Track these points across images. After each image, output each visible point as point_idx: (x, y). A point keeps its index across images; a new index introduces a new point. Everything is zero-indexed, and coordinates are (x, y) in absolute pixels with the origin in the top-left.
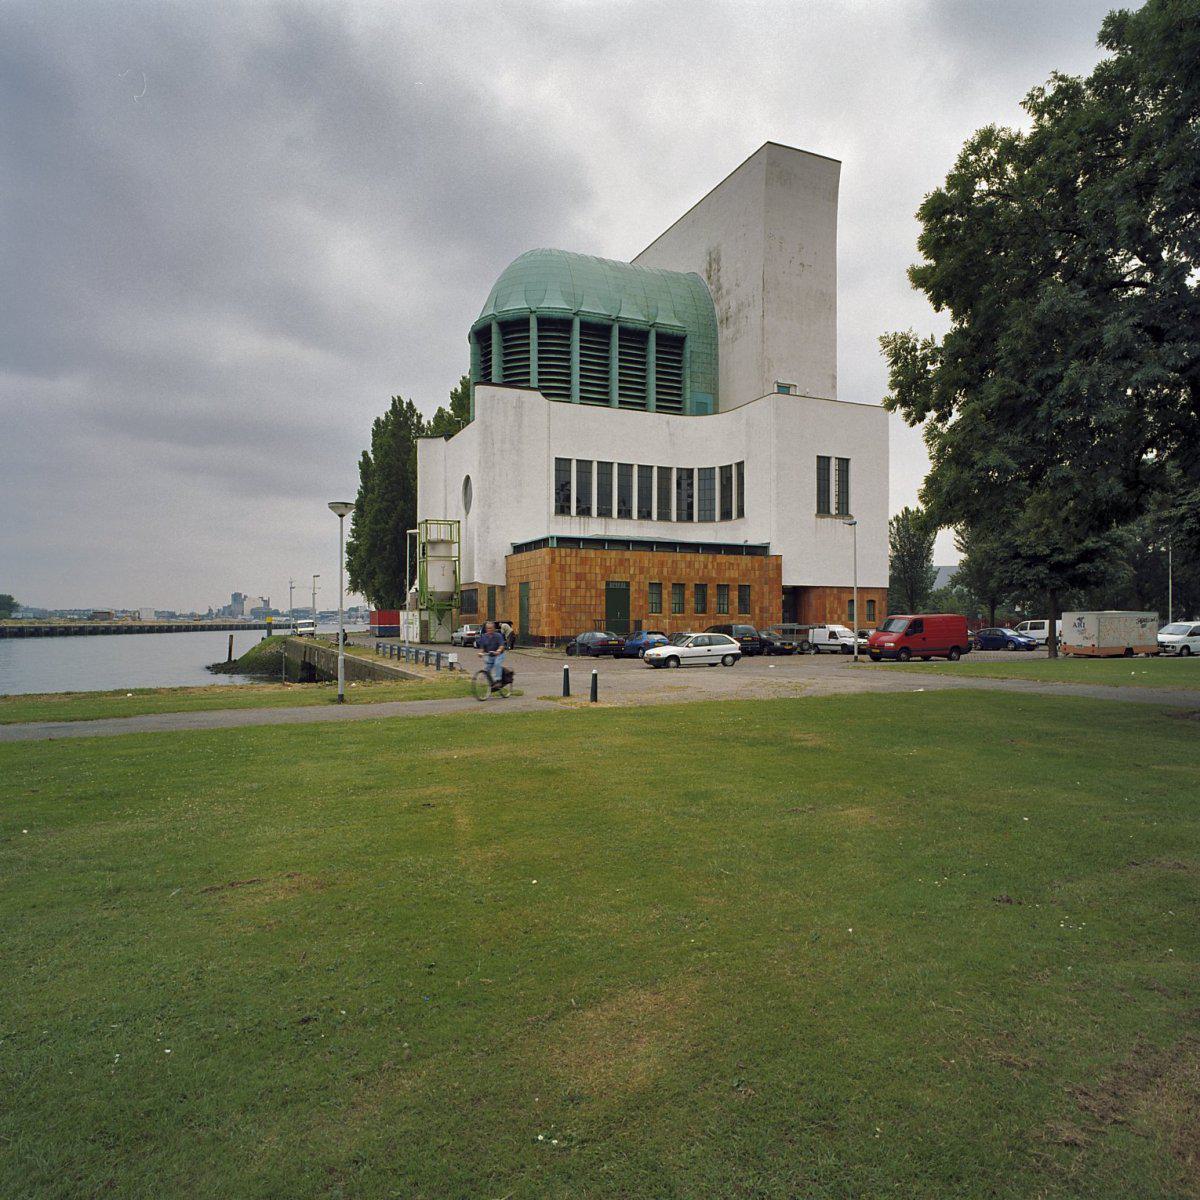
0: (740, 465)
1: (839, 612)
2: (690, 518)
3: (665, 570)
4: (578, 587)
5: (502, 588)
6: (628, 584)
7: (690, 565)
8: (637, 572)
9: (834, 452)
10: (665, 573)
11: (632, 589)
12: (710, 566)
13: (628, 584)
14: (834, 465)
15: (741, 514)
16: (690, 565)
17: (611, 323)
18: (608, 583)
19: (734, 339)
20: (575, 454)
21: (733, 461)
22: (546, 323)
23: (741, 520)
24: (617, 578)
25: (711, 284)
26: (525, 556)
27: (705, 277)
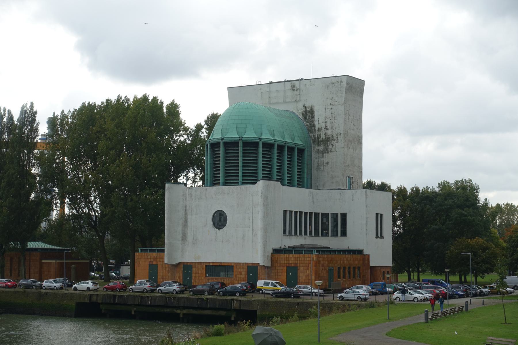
3: (341, 261)
5: (268, 267)
9: (379, 212)
14: (379, 215)
19: (323, 152)
20: (289, 209)
23: (343, 238)
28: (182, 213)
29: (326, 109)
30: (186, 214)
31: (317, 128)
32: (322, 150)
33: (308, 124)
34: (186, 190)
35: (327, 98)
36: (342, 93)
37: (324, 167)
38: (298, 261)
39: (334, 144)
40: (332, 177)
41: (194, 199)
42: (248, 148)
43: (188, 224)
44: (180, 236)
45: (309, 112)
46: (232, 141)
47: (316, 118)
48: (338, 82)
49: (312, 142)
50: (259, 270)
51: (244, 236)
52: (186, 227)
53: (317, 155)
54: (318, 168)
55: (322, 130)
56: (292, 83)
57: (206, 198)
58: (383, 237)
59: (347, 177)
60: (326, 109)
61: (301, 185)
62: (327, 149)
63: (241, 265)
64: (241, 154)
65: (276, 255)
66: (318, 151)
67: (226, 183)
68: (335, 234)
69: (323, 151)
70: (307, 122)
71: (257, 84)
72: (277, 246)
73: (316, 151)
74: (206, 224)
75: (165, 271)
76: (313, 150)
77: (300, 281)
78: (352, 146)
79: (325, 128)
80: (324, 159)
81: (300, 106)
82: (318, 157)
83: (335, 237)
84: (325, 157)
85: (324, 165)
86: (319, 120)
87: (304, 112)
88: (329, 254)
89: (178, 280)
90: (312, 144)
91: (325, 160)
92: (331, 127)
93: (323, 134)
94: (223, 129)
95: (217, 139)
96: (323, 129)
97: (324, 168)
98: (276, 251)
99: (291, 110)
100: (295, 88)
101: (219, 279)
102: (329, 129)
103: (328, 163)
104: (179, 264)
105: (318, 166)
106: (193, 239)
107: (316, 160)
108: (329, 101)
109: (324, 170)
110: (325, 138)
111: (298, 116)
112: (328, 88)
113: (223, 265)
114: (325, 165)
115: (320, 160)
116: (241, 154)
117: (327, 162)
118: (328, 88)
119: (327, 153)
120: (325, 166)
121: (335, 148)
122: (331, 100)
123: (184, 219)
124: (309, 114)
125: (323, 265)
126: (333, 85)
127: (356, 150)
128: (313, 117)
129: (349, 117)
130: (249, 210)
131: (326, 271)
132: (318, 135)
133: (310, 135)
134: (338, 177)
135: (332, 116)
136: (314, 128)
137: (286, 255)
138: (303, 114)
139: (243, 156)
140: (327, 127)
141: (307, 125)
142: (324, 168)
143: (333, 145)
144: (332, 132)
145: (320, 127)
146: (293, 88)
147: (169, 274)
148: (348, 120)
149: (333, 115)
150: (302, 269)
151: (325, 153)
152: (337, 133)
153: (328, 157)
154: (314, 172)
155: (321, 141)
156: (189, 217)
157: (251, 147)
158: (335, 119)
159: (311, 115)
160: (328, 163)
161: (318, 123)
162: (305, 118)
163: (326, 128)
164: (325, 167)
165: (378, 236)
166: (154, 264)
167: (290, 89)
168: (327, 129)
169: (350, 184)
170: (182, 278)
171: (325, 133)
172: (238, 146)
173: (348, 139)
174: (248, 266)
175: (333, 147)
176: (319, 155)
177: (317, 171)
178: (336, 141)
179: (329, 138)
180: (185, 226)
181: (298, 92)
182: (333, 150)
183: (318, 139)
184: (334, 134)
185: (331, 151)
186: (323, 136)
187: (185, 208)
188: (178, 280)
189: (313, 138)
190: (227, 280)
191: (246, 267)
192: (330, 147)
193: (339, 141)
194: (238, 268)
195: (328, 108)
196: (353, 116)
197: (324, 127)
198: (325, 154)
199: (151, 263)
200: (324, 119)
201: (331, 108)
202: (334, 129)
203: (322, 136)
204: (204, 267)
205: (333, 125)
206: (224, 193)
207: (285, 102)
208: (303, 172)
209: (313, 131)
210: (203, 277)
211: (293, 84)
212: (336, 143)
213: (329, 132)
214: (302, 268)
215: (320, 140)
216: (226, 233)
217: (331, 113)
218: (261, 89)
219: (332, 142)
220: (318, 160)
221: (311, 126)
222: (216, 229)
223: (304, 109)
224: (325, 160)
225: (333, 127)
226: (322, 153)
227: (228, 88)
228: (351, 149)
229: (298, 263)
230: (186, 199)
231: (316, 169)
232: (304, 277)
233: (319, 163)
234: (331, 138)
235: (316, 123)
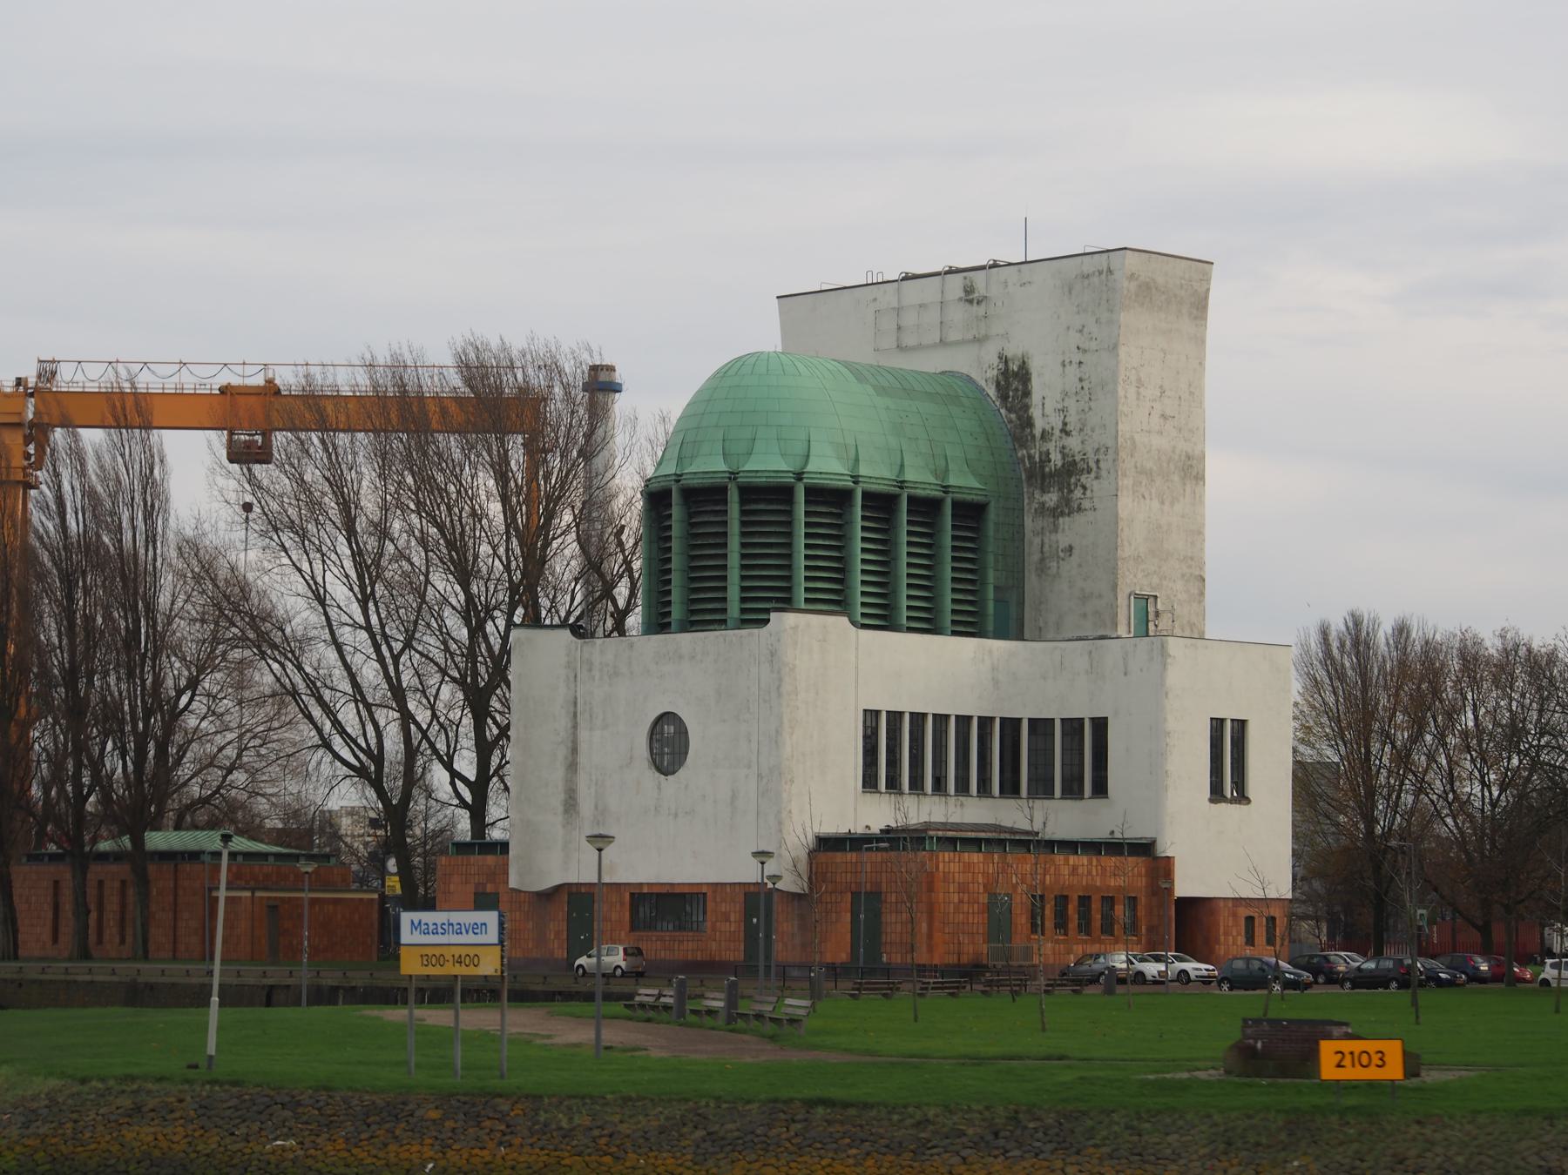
0: (1100, 725)
1: (1235, 934)
3: (1048, 877)
4: (961, 901)
9: (1229, 713)
10: (1048, 882)
12: (1094, 873)
16: (1075, 868)
19: (1056, 513)
20: (885, 705)
22: (817, 494)
23: (1099, 803)
28: (563, 723)
29: (1064, 366)
30: (575, 727)
31: (1037, 432)
32: (1052, 504)
33: (1013, 416)
34: (577, 649)
35: (1068, 328)
36: (1112, 311)
37: (1058, 562)
38: (884, 874)
39: (1088, 485)
40: (1085, 598)
41: (597, 678)
42: (761, 507)
43: (582, 759)
44: (557, 800)
45: (1016, 375)
46: (706, 485)
47: (1036, 397)
48: (1100, 273)
49: (1024, 477)
50: (777, 907)
51: (734, 797)
52: (576, 770)
53: (1040, 523)
54: (1042, 568)
55: (1054, 438)
56: (965, 278)
57: (632, 673)
59: (1130, 595)
60: (1064, 366)
61: (970, 626)
62: (1068, 502)
63: (737, 887)
64: (734, 528)
65: (823, 857)
66: (1042, 510)
67: (693, 623)
68: (1073, 789)
69: (1057, 507)
70: (1009, 410)
71: (870, 282)
72: (834, 826)
73: (1036, 510)
74: (631, 758)
75: (518, 913)
76: (1028, 504)
77: (889, 940)
78: (1153, 491)
79: (1061, 431)
80: (1060, 536)
81: (990, 355)
82: (1043, 528)
83: (1076, 799)
84: (1063, 529)
85: (1058, 557)
86: (1043, 404)
87: (1000, 378)
88: (977, 849)
89: (556, 941)
90: (1025, 485)
91: (1063, 540)
92: (1079, 426)
93: (1058, 449)
94: (685, 445)
95: (664, 479)
96: (1057, 432)
97: (1058, 568)
98: (827, 844)
99: (964, 371)
100: (976, 295)
101: (667, 938)
102: (1073, 433)
103: (1070, 549)
104: (558, 888)
105: (1042, 560)
106: (596, 807)
107: (1037, 541)
108: (1074, 339)
109: (1058, 573)
110: (1063, 465)
111: (984, 390)
112: (1070, 293)
113: (677, 891)
114: (1061, 554)
115: (1046, 541)
116: (734, 528)
117: (1067, 545)
118: (1070, 293)
119: (1069, 515)
120: (1063, 559)
121: (1092, 498)
122: (1078, 335)
123: (570, 745)
124: (1015, 384)
125: (963, 888)
126: (1086, 282)
127: (1172, 504)
128: (1027, 393)
129: (1141, 390)
130: (749, 708)
131: (976, 906)
132: (1041, 453)
133: (1020, 455)
134: (1100, 596)
135: (1082, 388)
136: (1031, 431)
137: (849, 855)
138: (998, 384)
139: (743, 534)
140: (1068, 428)
141: (1011, 421)
142: (1058, 568)
143: (1084, 488)
144: (1082, 442)
145: (1048, 428)
146: (970, 296)
147: (530, 925)
148: (1138, 399)
149: (1085, 385)
150: (894, 900)
151: (1062, 514)
152: (1096, 446)
153: (1071, 530)
154: (1031, 581)
155: (1051, 475)
156: (583, 735)
157: (770, 502)
158: (1093, 398)
159: (1020, 387)
160: (1070, 549)
161: (1041, 411)
162: (1004, 397)
163: (1065, 432)
164: (1061, 562)
165: (1225, 797)
166: (488, 890)
167: (960, 299)
168: (1068, 434)
169: (1148, 621)
170: (565, 936)
171: (1064, 447)
172: (725, 502)
173: (1136, 467)
174: (745, 894)
175: (1084, 494)
176: (1045, 525)
177: (1039, 576)
178: (1093, 475)
179: (1074, 463)
180: (572, 766)
181: (981, 310)
182: (1086, 504)
183: (1042, 468)
184: (1089, 450)
185: (1079, 509)
186: (1056, 459)
187: (572, 709)
188: (556, 941)
189: (1027, 465)
190: (690, 938)
191: (742, 897)
192: (1078, 493)
193: (1104, 473)
194: (718, 900)
195: (1071, 362)
196: (1161, 387)
197: (1060, 426)
198: (1061, 519)
199: (481, 890)
200: (1059, 397)
201: (1080, 363)
202: (1090, 433)
203: (1052, 457)
204: (627, 897)
205: (1086, 420)
206: (681, 657)
207: (943, 343)
208: (984, 583)
209: (1027, 440)
210: (623, 933)
211: (968, 282)
212: (1095, 483)
213: (1073, 443)
214: (894, 895)
215: (1047, 470)
216: (686, 787)
217: (1081, 380)
218: (875, 300)
219: (1083, 479)
220: (1042, 540)
221: (1021, 425)
222: (657, 774)
223: (1002, 366)
224: (1063, 540)
225: (1084, 425)
226: (1054, 516)
227: (778, 297)
228: (1151, 499)
229: (884, 880)
230: (576, 676)
231: (1037, 569)
232: (899, 926)
233: (1045, 550)
234: (1081, 465)
235: (1035, 412)
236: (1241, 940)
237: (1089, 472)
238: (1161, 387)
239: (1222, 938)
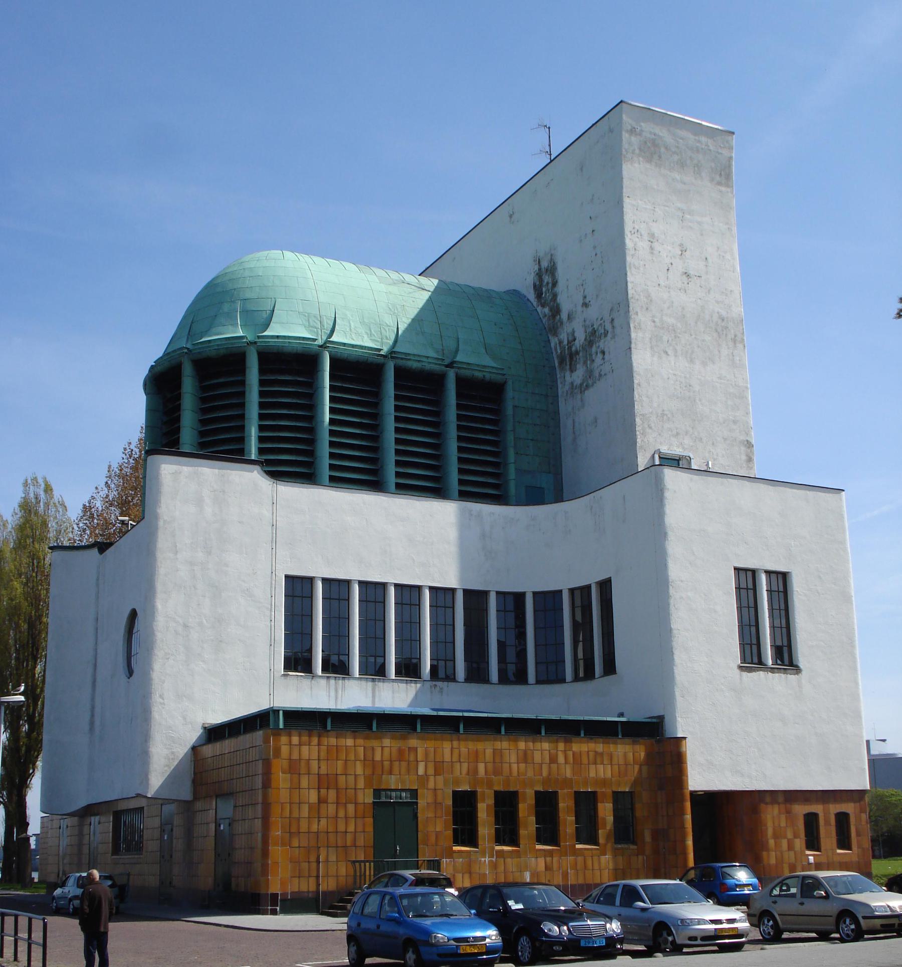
0: (605, 586)
1: (790, 835)
2: (521, 678)
3: (481, 767)
4: (321, 801)
6: (414, 793)
7: (525, 757)
8: (431, 771)
11: (422, 803)
12: (561, 759)
13: (414, 793)
15: (610, 668)
16: (525, 757)
17: (381, 360)
18: (377, 793)
19: (584, 387)
21: (590, 577)
24: (393, 782)
25: (543, 306)
26: (227, 745)
27: (531, 296)
42: (221, 380)
58: (797, 666)
65: (209, 750)
136: (560, 318)
151: (587, 387)
160: (596, 420)
182: (606, 368)
183: (570, 348)
192: (598, 359)
196: (681, 245)
197: (581, 302)
213: (592, 313)
223: (537, 267)
228: (676, 356)
236: (800, 843)
237: (606, 335)
238: (681, 245)
239: (772, 842)
